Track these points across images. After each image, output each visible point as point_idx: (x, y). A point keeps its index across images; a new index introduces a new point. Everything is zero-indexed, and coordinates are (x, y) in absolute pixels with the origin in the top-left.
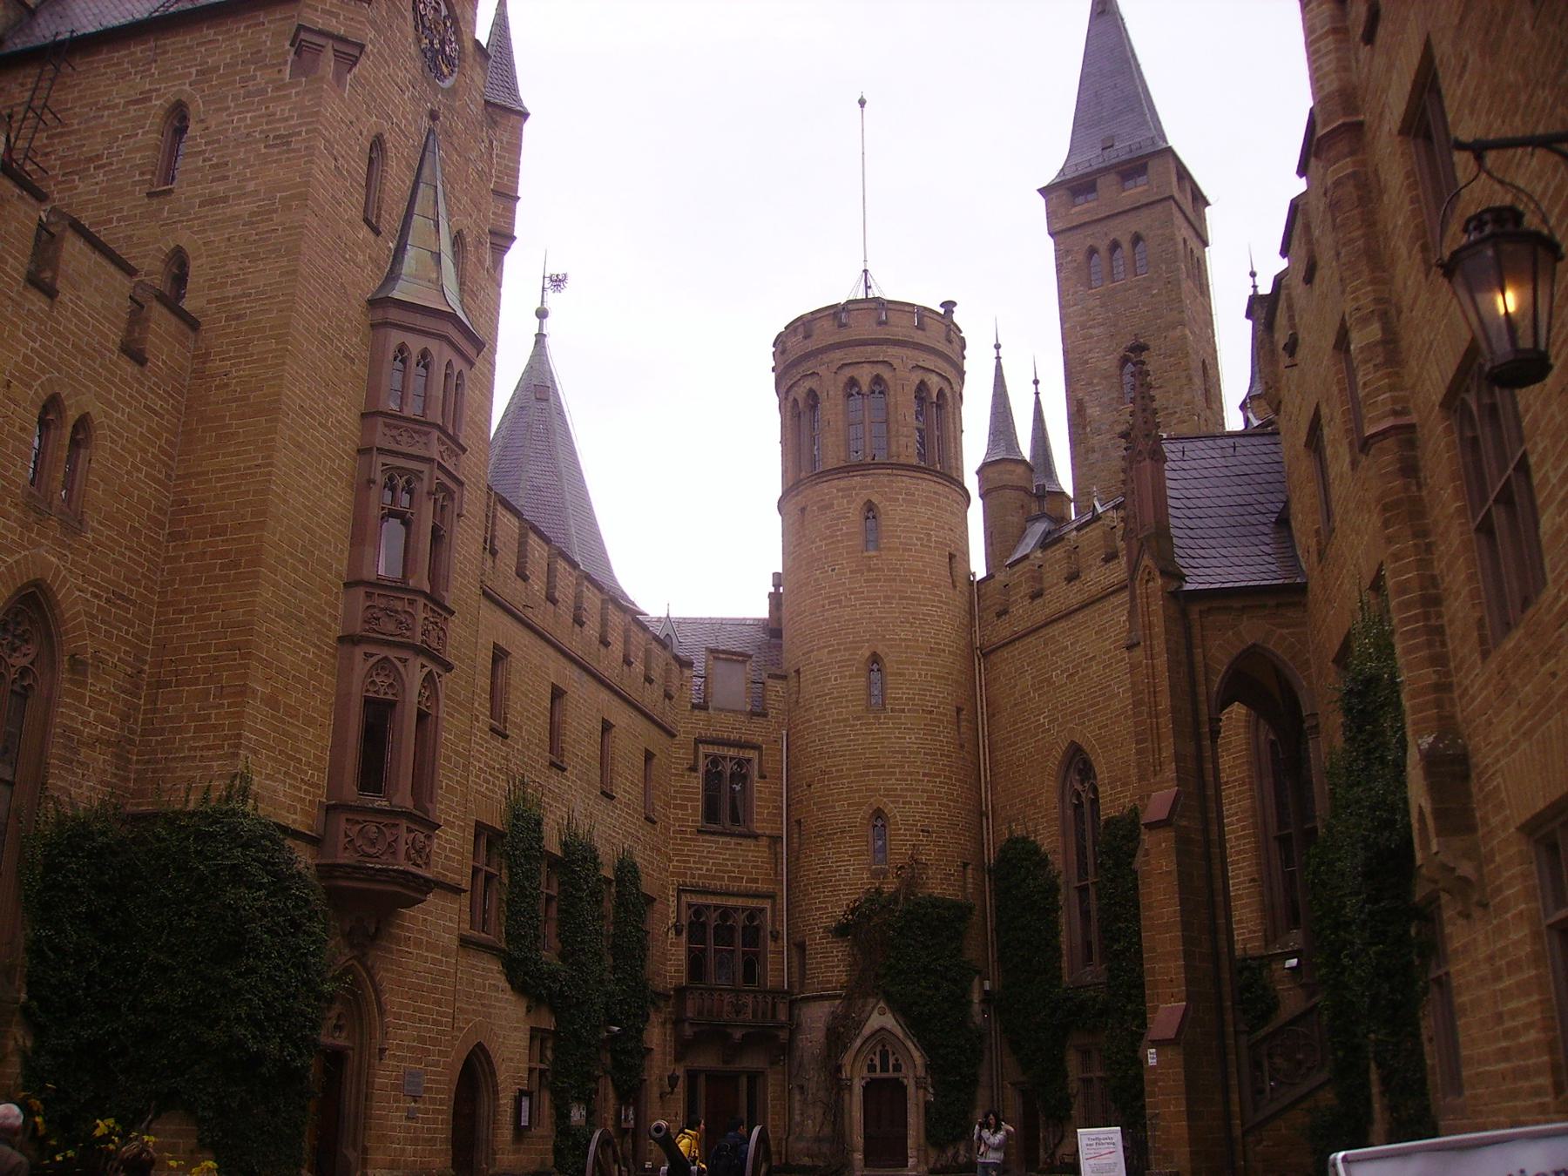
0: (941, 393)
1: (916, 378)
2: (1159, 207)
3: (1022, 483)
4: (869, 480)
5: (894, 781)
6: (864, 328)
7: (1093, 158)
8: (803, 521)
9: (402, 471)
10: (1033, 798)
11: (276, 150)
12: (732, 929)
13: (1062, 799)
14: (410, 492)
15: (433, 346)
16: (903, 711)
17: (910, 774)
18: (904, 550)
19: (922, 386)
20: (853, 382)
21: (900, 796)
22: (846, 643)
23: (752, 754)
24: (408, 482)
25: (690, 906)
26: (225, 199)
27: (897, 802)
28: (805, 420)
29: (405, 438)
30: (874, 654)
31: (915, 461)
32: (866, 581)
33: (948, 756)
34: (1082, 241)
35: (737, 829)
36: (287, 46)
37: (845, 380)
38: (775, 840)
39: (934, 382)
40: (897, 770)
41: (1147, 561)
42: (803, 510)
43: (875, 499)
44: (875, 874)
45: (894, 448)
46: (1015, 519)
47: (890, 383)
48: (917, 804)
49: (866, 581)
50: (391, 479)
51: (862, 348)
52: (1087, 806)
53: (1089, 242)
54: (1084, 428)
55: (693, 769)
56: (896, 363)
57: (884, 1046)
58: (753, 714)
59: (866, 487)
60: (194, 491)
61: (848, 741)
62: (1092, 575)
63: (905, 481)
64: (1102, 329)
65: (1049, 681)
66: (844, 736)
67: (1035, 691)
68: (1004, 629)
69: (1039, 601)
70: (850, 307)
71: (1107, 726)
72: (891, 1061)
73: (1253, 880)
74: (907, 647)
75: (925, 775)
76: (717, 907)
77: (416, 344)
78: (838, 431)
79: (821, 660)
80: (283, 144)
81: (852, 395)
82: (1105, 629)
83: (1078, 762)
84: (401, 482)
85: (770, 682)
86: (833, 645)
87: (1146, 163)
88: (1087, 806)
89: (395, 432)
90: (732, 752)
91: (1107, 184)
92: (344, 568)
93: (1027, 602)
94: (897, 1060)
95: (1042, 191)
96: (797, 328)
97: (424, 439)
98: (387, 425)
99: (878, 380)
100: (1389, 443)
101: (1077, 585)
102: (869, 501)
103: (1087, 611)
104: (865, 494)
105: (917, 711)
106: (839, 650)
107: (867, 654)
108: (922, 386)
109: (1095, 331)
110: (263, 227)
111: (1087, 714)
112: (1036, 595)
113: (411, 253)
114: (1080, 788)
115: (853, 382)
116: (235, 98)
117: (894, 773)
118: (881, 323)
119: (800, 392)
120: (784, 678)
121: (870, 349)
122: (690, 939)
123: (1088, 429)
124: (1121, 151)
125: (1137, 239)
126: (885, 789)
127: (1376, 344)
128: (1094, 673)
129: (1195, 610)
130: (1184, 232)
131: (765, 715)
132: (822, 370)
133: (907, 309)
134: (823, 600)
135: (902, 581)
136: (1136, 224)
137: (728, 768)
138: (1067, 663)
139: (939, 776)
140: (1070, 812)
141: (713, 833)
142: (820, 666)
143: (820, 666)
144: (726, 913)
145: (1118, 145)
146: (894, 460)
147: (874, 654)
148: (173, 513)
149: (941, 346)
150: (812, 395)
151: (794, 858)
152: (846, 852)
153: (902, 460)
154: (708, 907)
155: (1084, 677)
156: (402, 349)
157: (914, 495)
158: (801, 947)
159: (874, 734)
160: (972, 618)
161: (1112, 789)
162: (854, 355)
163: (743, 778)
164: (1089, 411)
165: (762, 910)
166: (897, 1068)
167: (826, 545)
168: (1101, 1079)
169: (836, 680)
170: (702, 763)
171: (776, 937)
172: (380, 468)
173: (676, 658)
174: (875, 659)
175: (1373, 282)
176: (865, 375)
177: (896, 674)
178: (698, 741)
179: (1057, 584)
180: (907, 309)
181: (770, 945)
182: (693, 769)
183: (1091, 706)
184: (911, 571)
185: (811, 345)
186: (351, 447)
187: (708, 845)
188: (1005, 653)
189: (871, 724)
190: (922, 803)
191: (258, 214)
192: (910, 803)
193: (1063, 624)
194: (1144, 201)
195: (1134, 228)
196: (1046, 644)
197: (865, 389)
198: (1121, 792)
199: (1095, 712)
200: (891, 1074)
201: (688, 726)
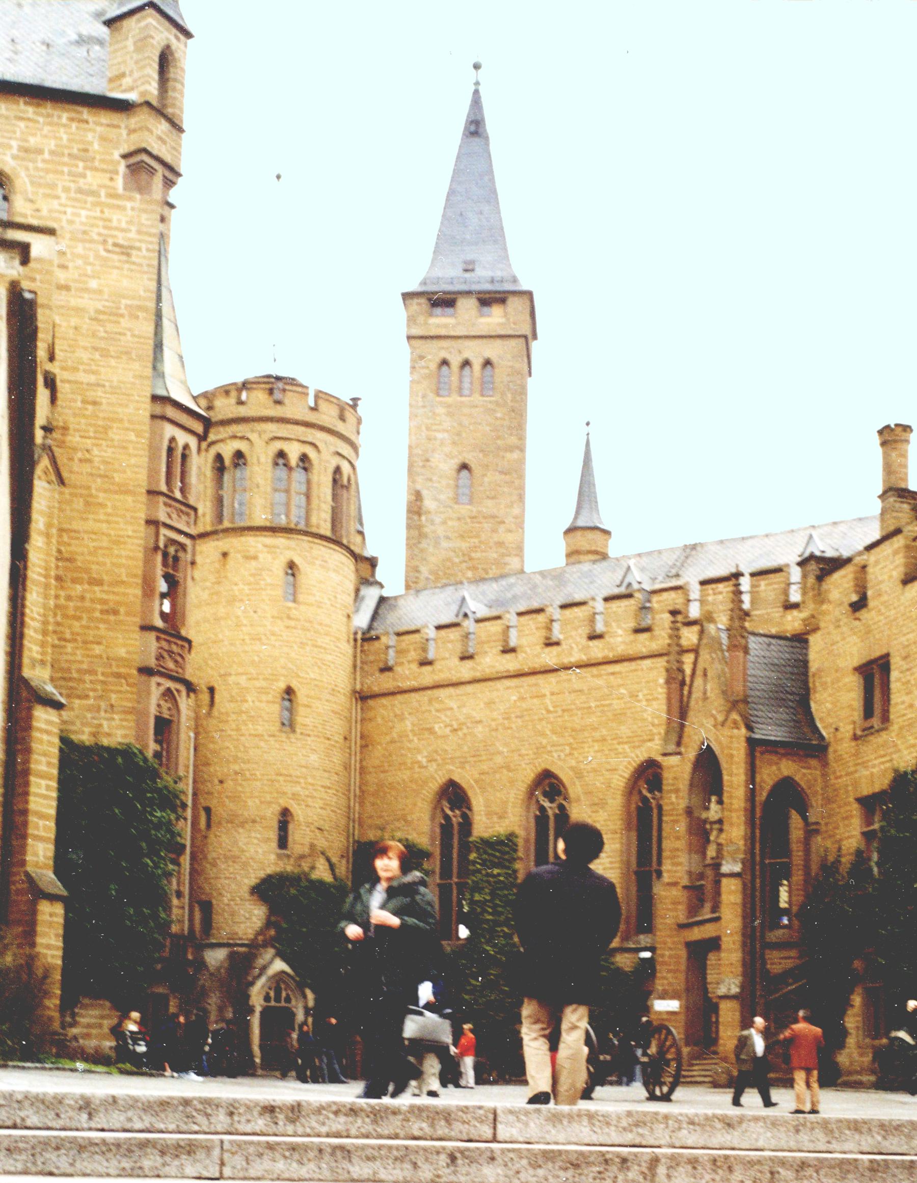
9: (173, 542)
11: (115, 257)
14: (176, 559)
24: (176, 551)
26: (67, 288)
29: (174, 516)
36: (116, 155)
39: (346, 468)
50: (166, 546)
68: (386, 682)
77: (182, 438)
80: (123, 253)
84: (172, 550)
89: (169, 510)
98: (165, 504)
110: (110, 327)
116: (66, 190)
149: (353, 437)
156: (173, 440)
160: (355, 666)
188: (384, 701)
191: (104, 313)
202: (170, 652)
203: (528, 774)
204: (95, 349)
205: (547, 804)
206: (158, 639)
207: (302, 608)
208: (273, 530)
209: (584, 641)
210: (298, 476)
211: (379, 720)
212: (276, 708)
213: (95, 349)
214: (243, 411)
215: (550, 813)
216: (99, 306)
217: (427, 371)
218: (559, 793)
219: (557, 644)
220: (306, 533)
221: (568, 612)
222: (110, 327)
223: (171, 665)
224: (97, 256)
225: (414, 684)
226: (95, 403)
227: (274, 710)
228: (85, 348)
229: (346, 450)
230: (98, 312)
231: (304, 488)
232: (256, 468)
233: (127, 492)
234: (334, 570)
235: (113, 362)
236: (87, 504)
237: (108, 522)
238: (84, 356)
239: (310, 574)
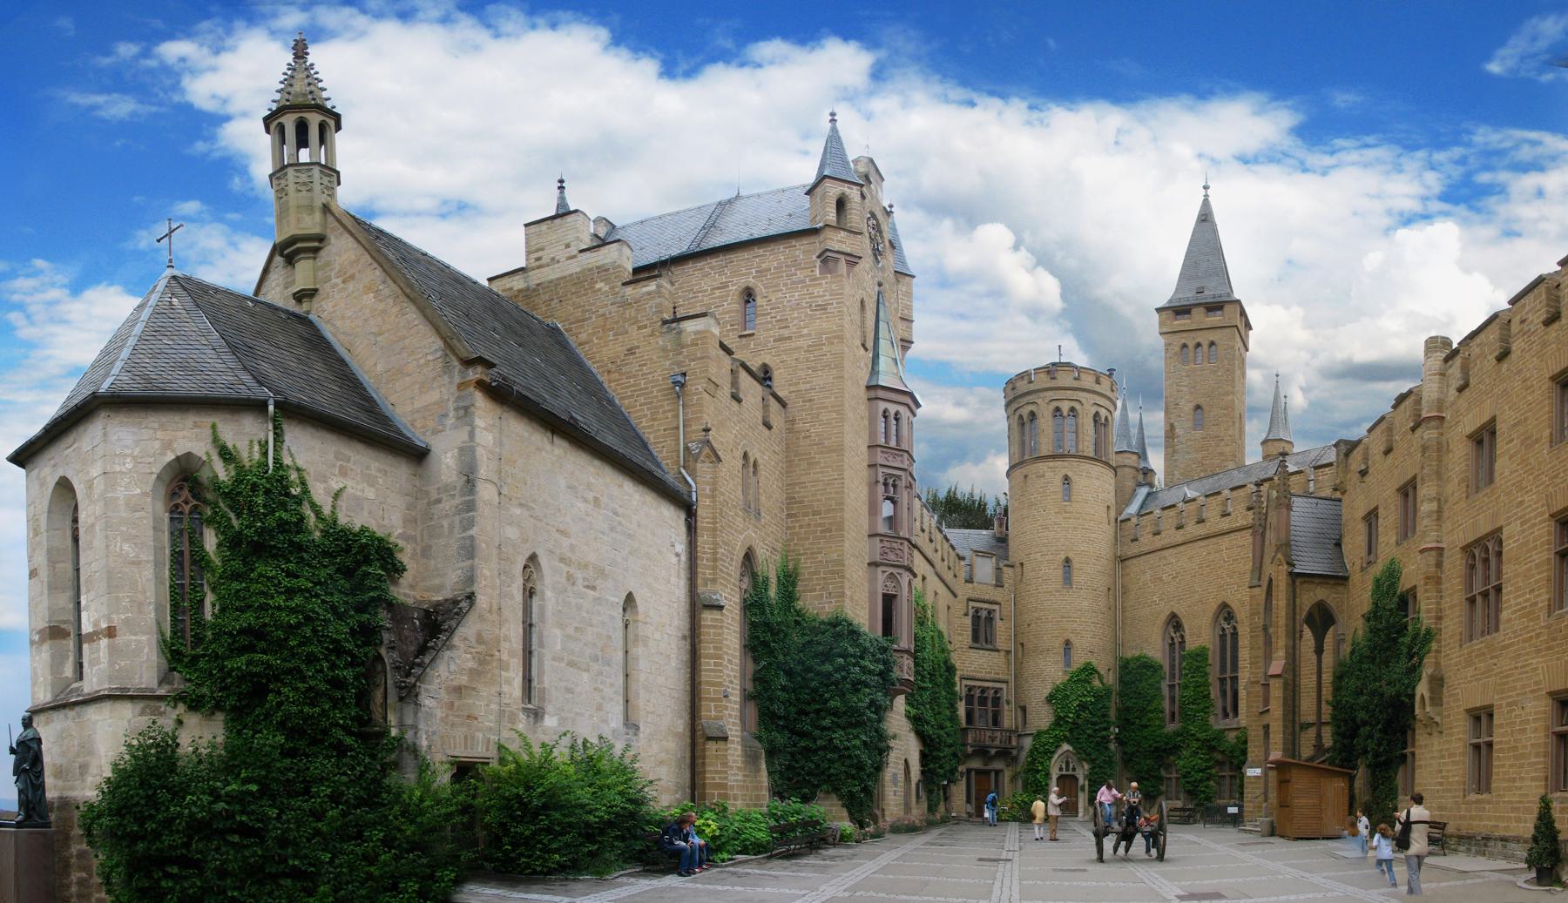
0: (1106, 419)
1: (1094, 410)
2: (1227, 330)
3: (1136, 465)
4: (1066, 464)
6: (1064, 379)
7: (1189, 296)
12: (986, 698)
13: (1163, 639)
14: (894, 486)
15: (903, 410)
19: (1097, 414)
20: (1058, 409)
23: (996, 607)
25: (966, 686)
28: (1027, 427)
31: (1092, 455)
34: (1179, 340)
35: (989, 647)
38: (1008, 652)
41: (1280, 556)
42: (1026, 476)
43: (1070, 474)
45: (1080, 447)
46: (1130, 484)
47: (1080, 411)
50: (886, 479)
52: (1177, 645)
55: (966, 615)
56: (1084, 401)
58: (997, 586)
59: (1064, 467)
60: (798, 492)
63: (1086, 466)
65: (1160, 579)
68: (1134, 549)
76: (979, 687)
77: (892, 408)
83: (1175, 622)
84: (890, 481)
85: (1005, 569)
88: (1177, 645)
89: (886, 455)
90: (986, 606)
92: (866, 527)
97: (900, 458)
99: (1072, 409)
101: (1181, 531)
102: (1066, 475)
104: (1064, 471)
108: (1097, 414)
112: (1157, 533)
113: (882, 360)
114: (1174, 635)
118: (1075, 379)
119: (1025, 412)
120: (1012, 566)
121: (1069, 392)
122: (966, 704)
130: (1240, 344)
131: (1002, 586)
132: (1039, 401)
136: (1212, 336)
137: (984, 614)
140: (1167, 647)
141: (977, 648)
144: (984, 690)
146: (1080, 454)
148: (788, 504)
150: (1033, 415)
151: (1019, 664)
153: (1085, 454)
154: (975, 687)
158: (1024, 709)
162: (1059, 394)
163: (990, 619)
165: (1001, 689)
170: (971, 612)
171: (1008, 702)
172: (880, 474)
173: (958, 555)
174: (1067, 560)
176: (1065, 407)
178: (969, 600)
181: (1006, 707)
182: (966, 615)
186: (866, 464)
187: (974, 654)
188: (1134, 561)
193: (1171, 550)
195: (1211, 339)
201: (964, 591)
202: (892, 549)
203: (1213, 606)
204: (809, 368)
205: (1226, 626)
206: (881, 541)
207: (1074, 505)
208: (1053, 457)
209: (1245, 512)
210: (1069, 421)
211: (1132, 575)
212: (1060, 572)
213: (809, 368)
214: (1032, 387)
215: (1227, 631)
216: (810, 342)
218: (1232, 618)
219: (1229, 514)
221: (1235, 493)
222: (816, 353)
223: (892, 557)
224: (807, 315)
225: (1151, 548)
226: (810, 400)
228: (803, 370)
230: (809, 346)
231: (1074, 428)
232: (1042, 421)
233: (833, 451)
235: (820, 373)
236: (809, 464)
237: (822, 472)
238: (803, 374)
239: (1079, 483)
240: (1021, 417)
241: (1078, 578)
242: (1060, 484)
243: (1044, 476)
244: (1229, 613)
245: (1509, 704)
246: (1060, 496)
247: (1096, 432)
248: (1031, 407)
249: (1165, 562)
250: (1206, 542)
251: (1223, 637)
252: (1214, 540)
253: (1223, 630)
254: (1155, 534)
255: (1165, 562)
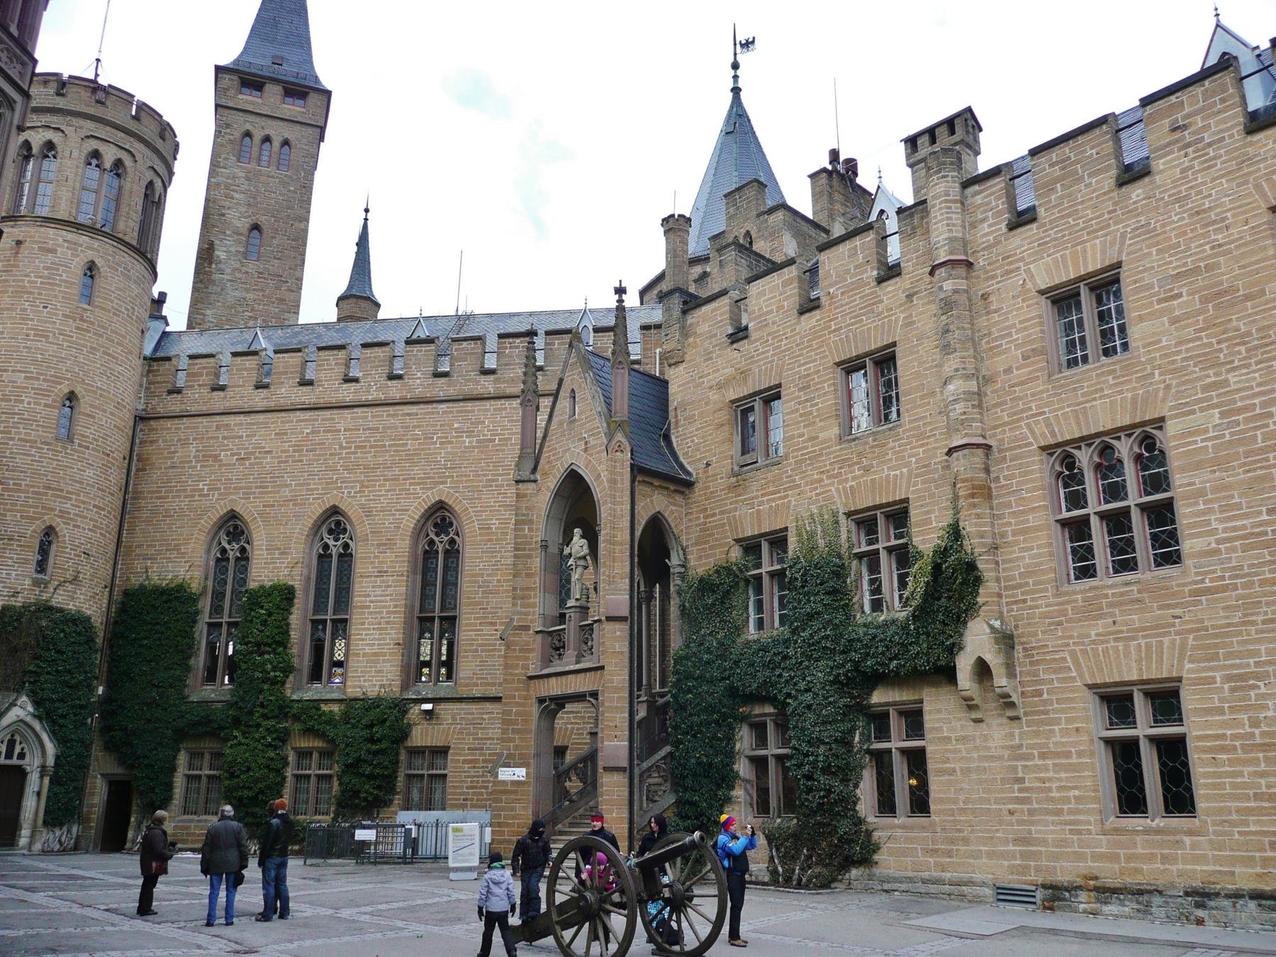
1: (149, 175)
4: (96, 244)
5: (68, 505)
8: (17, 253)
10: (176, 545)
13: (208, 551)
16: (88, 448)
17: (84, 502)
18: (114, 314)
20: (96, 154)
21: (72, 519)
22: (46, 375)
27: (69, 524)
30: (72, 393)
31: (134, 243)
32: (77, 328)
33: (112, 495)
37: (90, 149)
39: (158, 184)
40: (74, 497)
43: (97, 261)
44: (36, 583)
48: (84, 529)
49: (77, 328)
51: (114, 131)
53: (248, 127)
54: (211, 263)
56: (138, 157)
57: (13, 736)
59: (93, 249)
61: (32, 461)
62: (283, 390)
64: (242, 196)
65: (216, 458)
66: (29, 455)
67: (198, 461)
68: (174, 405)
69: (221, 394)
70: (111, 90)
71: (273, 506)
72: (17, 750)
73: (399, 644)
74: (101, 395)
75: (95, 506)
78: (74, 188)
79: (16, 382)
81: (48, 157)
82: (286, 434)
86: (32, 372)
87: (308, 93)
91: (272, 92)
93: (205, 391)
94: (22, 749)
95: (219, 70)
96: (49, 81)
99: (118, 163)
100: (980, 451)
101: (263, 393)
102: (93, 262)
103: (269, 415)
104: (91, 255)
105: (99, 451)
106: (38, 379)
107: (66, 391)
109: (236, 195)
111: (254, 493)
114: (227, 546)
115: (96, 154)
117: (70, 499)
123: (214, 266)
124: (289, 70)
125: (286, 143)
126: (60, 511)
127: (974, 393)
128: (267, 463)
129: (639, 478)
133: (156, 117)
134: (27, 329)
135: (107, 339)
138: (238, 449)
139: (104, 509)
140: (212, 563)
142: (13, 387)
143: (13, 387)
145: (285, 67)
147: (72, 393)
149: (169, 158)
152: (12, 558)
153: (127, 239)
155: (257, 464)
157: (129, 271)
159: (59, 461)
161: (268, 554)
162: (103, 131)
164: (217, 253)
166: (22, 756)
167: (42, 283)
168: (209, 777)
169: (29, 403)
174: (71, 397)
175: (975, 357)
176: (110, 154)
177: (89, 415)
179: (243, 386)
180: (156, 117)
183: (256, 488)
184: (116, 333)
185: (61, 103)
188: (169, 423)
189: (57, 451)
190: (89, 530)
192: (78, 527)
193: (242, 417)
194: (299, 119)
196: (218, 428)
197: (108, 165)
198: (279, 559)
199: (261, 493)
200: (15, 761)
217: (232, 137)
220: (110, 236)
225: (204, 409)
227: (49, 414)
229: (161, 169)
234: (135, 282)
240: (27, 145)
241: (85, 429)
242: (80, 273)
243: (53, 251)
244: (338, 523)
245: (1229, 678)
246: (76, 291)
247: (144, 210)
248: (50, 135)
249: (226, 433)
250: (308, 415)
251: (324, 557)
252: (327, 413)
253: (326, 547)
254: (213, 389)
255: (226, 433)
